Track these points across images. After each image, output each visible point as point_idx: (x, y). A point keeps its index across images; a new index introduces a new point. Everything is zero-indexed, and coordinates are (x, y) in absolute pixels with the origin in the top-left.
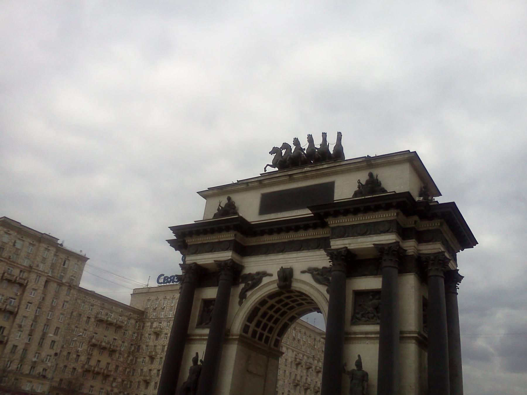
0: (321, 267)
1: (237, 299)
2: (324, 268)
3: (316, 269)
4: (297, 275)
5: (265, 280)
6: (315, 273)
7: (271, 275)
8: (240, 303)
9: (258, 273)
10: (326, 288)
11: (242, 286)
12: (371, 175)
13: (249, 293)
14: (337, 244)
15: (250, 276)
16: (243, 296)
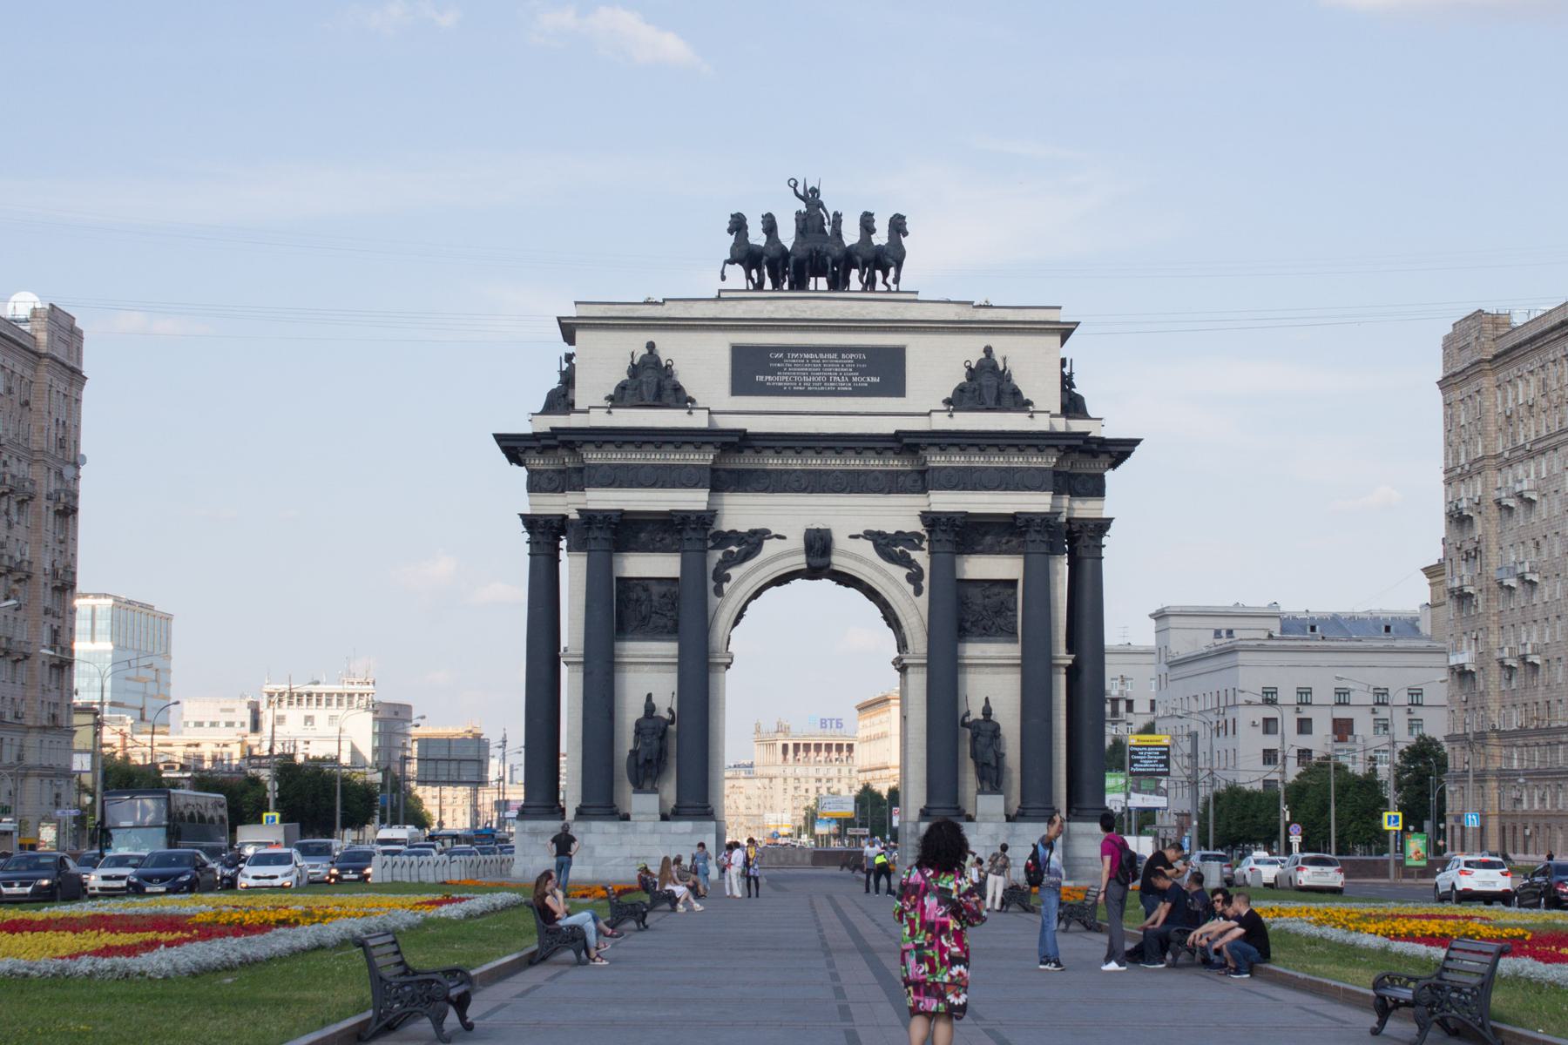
0: (891, 530)
1: (711, 584)
2: (898, 533)
3: (880, 534)
4: (840, 541)
5: (770, 547)
6: (880, 541)
7: (783, 538)
8: (719, 592)
9: (754, 533)
10: (905, 571)
11: (719, 554)
12: (988, 351)
13: (735, 572)
14: (946, 501)
15: (733, 536)
16: (721, 578)
